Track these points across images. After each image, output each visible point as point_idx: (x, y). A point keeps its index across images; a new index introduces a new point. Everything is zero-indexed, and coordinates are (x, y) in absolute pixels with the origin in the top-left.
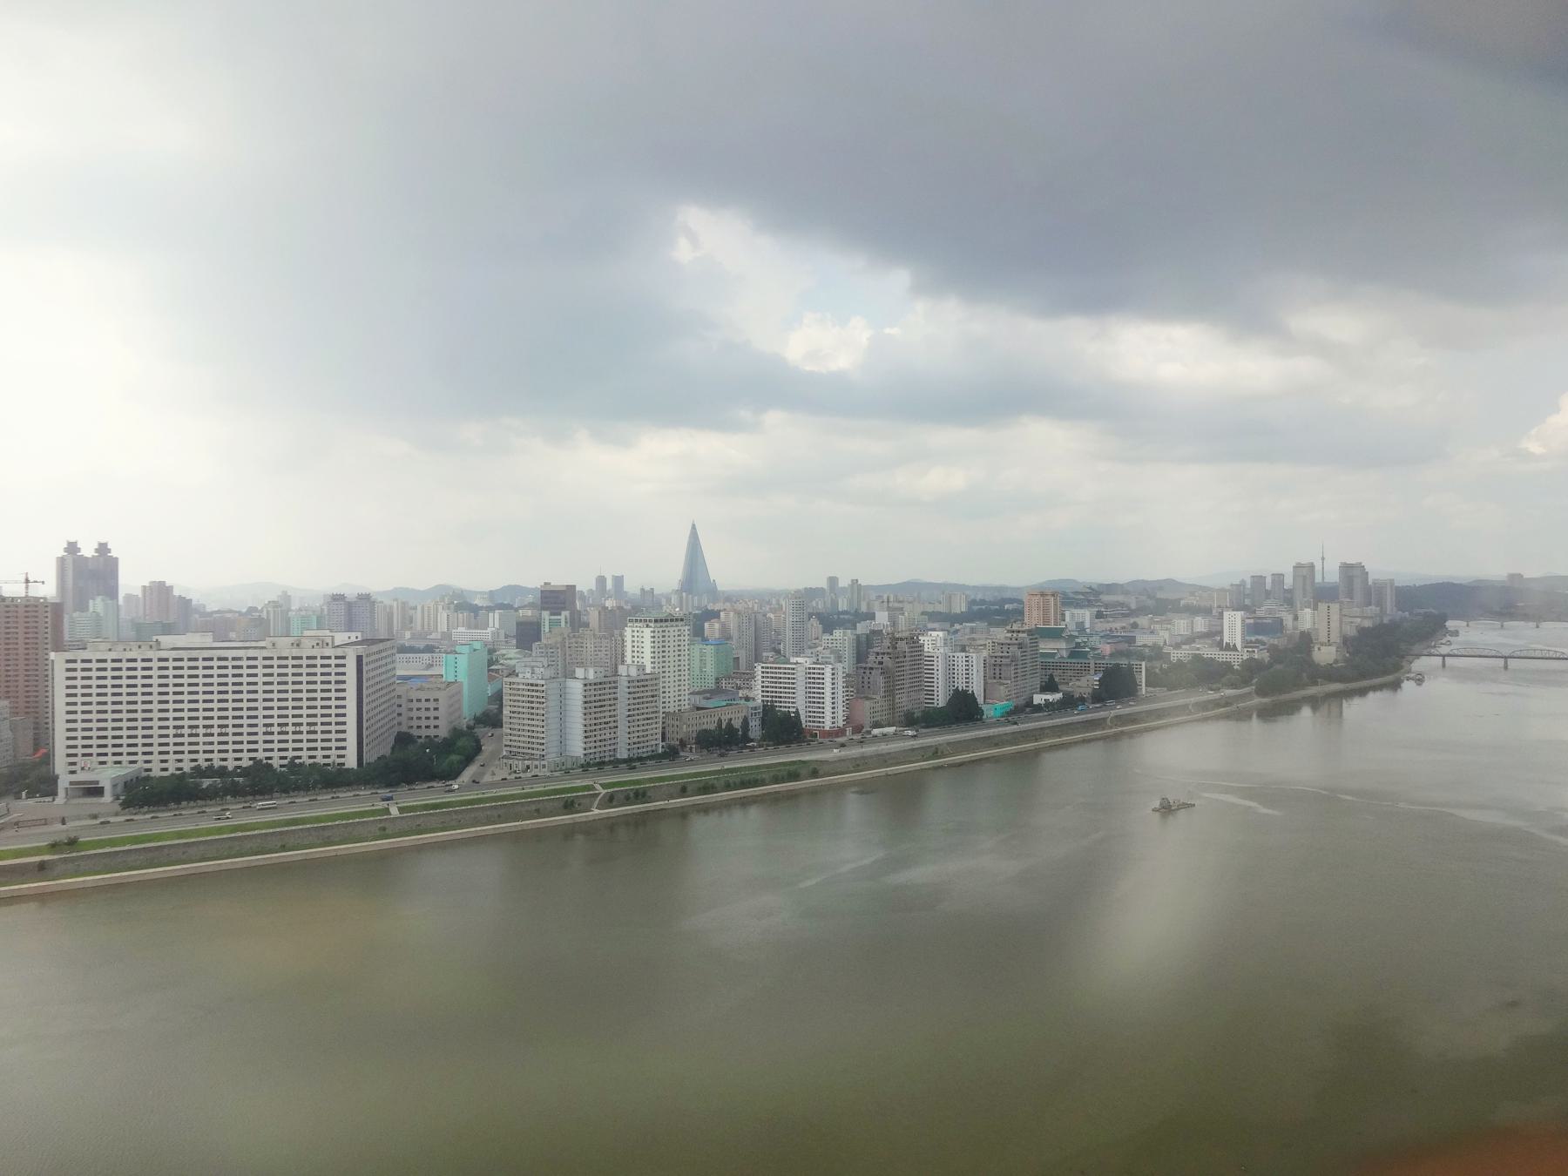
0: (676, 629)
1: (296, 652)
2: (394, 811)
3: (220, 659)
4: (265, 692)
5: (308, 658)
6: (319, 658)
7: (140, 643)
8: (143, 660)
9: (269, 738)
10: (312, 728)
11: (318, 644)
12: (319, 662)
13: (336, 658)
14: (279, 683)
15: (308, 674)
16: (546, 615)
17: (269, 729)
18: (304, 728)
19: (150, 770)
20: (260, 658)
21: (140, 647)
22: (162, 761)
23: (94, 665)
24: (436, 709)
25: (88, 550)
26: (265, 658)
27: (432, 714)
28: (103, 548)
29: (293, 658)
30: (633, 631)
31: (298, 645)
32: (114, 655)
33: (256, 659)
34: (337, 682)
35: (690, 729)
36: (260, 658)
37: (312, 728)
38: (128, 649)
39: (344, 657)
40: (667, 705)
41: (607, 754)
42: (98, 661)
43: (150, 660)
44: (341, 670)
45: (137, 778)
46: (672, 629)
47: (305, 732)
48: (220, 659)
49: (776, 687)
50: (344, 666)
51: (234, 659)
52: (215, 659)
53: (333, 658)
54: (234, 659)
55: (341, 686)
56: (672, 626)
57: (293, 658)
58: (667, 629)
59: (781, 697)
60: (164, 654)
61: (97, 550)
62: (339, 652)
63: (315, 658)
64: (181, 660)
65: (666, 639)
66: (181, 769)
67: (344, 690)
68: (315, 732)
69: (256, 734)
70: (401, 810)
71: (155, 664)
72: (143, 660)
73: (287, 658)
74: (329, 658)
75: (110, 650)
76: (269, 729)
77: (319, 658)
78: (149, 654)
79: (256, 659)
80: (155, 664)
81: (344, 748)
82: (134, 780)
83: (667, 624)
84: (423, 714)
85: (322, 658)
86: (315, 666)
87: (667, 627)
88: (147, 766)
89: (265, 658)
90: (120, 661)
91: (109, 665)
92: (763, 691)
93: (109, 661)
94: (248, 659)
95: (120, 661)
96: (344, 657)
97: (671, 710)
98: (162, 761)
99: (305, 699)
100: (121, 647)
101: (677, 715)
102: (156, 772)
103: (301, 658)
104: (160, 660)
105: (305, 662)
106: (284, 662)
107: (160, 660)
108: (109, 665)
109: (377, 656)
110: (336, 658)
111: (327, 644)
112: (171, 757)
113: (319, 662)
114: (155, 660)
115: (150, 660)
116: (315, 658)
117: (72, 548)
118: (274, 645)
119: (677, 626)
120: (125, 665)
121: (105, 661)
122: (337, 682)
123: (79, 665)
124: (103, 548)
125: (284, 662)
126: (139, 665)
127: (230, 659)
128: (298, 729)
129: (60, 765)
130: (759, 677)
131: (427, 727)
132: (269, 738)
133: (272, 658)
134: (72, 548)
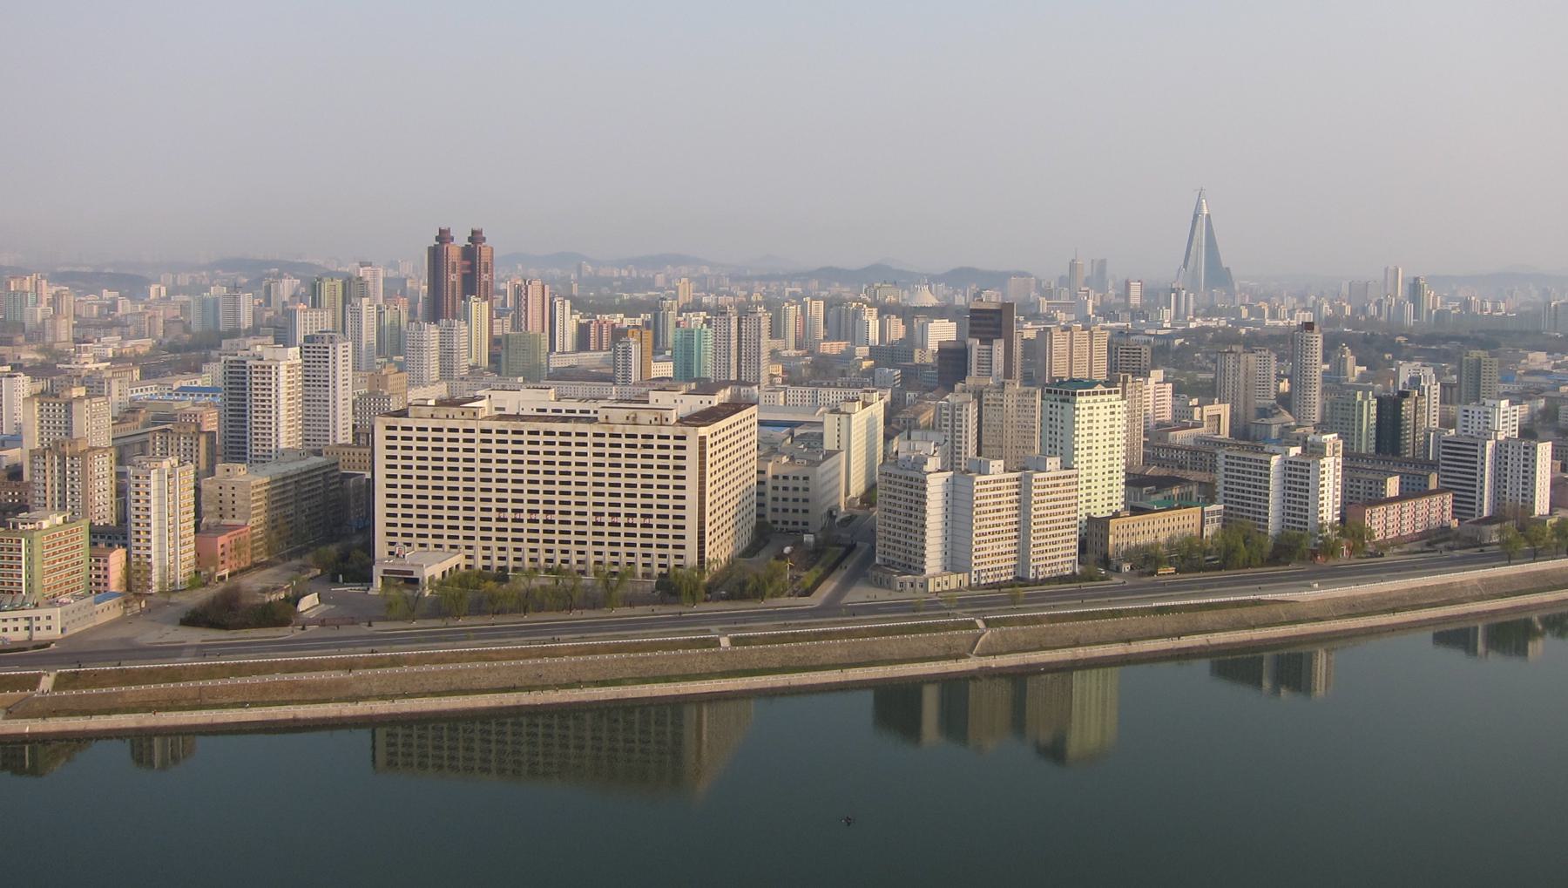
0: (1108, 404)
1: (630, 430)
2: (725, 642)
3: (546, 433)
4: (595, 474)
5: (644, 437)
6: (655, 437)
7: (463, 410)
8: (466, 431)
9: (599, 529)
10: (647, 521)
11: (656, 419)
12: (655, 442)
13: (676, 438)
14: (611, 465)
15: (643, 456)
16: (975, 344)
17: (599, 519)
18: (638, 521)
20: (590, 435)
24: (806, 489)
26: (596, 435)
27: (800, 495)
28: (476, 237)
29: (628, 436)
30: (1051, 406)
31: (635, 418)
32: (431, 424)
33: (585, 435)
34: (676, 467)
35: (1120, 541)
36: (590, 435)
37: (647, 521)
38: (450, 416)
39: (684, 438)
40: (1092, 504)
41: (1003, 572)
42: (419, 429)
43: (472, 431)
44: (680, 453)
46: (1102, 405)
47: (639, 526)
48: (546, 433)
49: (1243, 485)
50: (683, 448)
51: (562, 434)
52: (541, 433)
53: (672, 438)
54: (562, 434)
55: (681, 473)
56: (1103, 401)
57: (628, 436)
58: (1095, 405)
59: (1249, 505)
60: (487, 425)
62: (679, 431)
63: (652, 437)
64: (505, 432)
65: (1095, 425)
67: (683, 478)
68: (650, 526)
69: (585, 523)
70: (734, 642)
71: (477, 436)
72: (466, 431)
73: (619, 436)
74: (667, 438)
76: (599, 519)
77: (655, 437)
79: (585, 435)
80: (477, 436)
81: (683, 547)
83: (1095, 397)
84: (790, 495)
85: (660, 437)
86: (651, 447)
87: (1095, 401)
89: (596, 435)
90: (441, 430)
92: (1226, 489)
93: (430, 430)
94: (578, 434)
95: (441, 430)
96: (684, 438)
97: (1099, 515)
99: (639, 486)
100: (443, 412)
101: (1104, 522)
103: (635, 436)
104: (483, 431)
105: (640, 441)
106: (616, 441)
107: (483, 431)
109: (727, 433)
110: (676, 438)
111: (667, 420)
113: (655, 442)
114: (477, 431)
115: (472, 431)
116: (652, 437)
118: (607, 417)
119: (1110, 400)
122: (676, 467)
125: (616, 441)
127: (557, 434)
128: (631, 521)
130: (1222, 469)
131: (795, 511)
132: (599, 529)
133: (603, 435)
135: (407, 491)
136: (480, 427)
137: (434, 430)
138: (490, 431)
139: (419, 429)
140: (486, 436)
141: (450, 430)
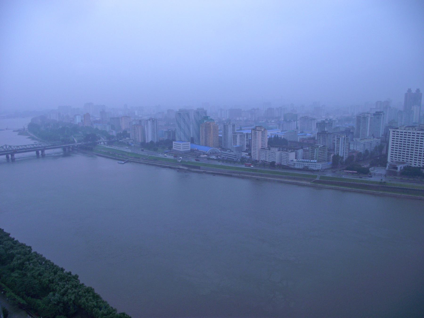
19: (411, 164)
21: (412, 129)
22: (415, 162)
23: (400, 133)
25: (414, 91)
28: (418, 90)
32: (405, 131)
38: (409, 129)
42: (401, 132)
43: (414, 133)
45: (407, 166)
60: (418, 132)
61: (416, 91)
66: (420, 165)
75: (404, 129)
78: (414, 132)
80: (416, 135)
82: (407, 166)
88: (411, 163)
90: (406, 133)
91: (404, 134)
95: (406, 133)
98: (415, 162)
100: (407, 129)
102: (413, 165)
104: (417, 133)
107: (417, 133)
108: (404, 134)
112: (417, 161)
114: (416, 133)
115: (414, 133)
117: (409, 90)
120: (408, 134)
121: (403, 132)
123: (396, 133)
124: (418, 90)
126: (411, 134)
129: (389, 160)
134: (409, 90)
135: (397, 147)
136: (417, 132)
137: (405, 132)
138: (419, 134)
139: (401, 132)
140: (418, 135)
141: (409, 133)
